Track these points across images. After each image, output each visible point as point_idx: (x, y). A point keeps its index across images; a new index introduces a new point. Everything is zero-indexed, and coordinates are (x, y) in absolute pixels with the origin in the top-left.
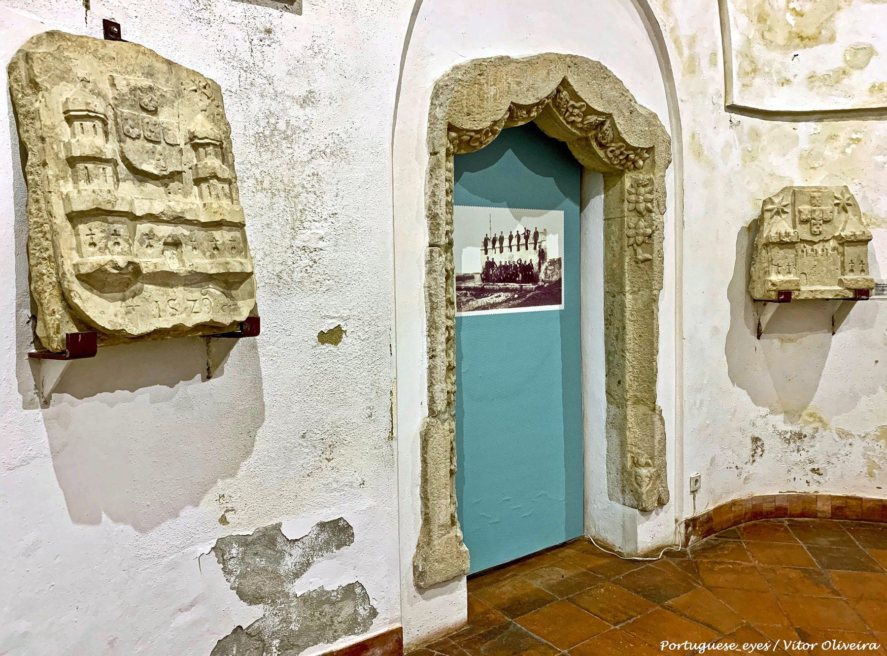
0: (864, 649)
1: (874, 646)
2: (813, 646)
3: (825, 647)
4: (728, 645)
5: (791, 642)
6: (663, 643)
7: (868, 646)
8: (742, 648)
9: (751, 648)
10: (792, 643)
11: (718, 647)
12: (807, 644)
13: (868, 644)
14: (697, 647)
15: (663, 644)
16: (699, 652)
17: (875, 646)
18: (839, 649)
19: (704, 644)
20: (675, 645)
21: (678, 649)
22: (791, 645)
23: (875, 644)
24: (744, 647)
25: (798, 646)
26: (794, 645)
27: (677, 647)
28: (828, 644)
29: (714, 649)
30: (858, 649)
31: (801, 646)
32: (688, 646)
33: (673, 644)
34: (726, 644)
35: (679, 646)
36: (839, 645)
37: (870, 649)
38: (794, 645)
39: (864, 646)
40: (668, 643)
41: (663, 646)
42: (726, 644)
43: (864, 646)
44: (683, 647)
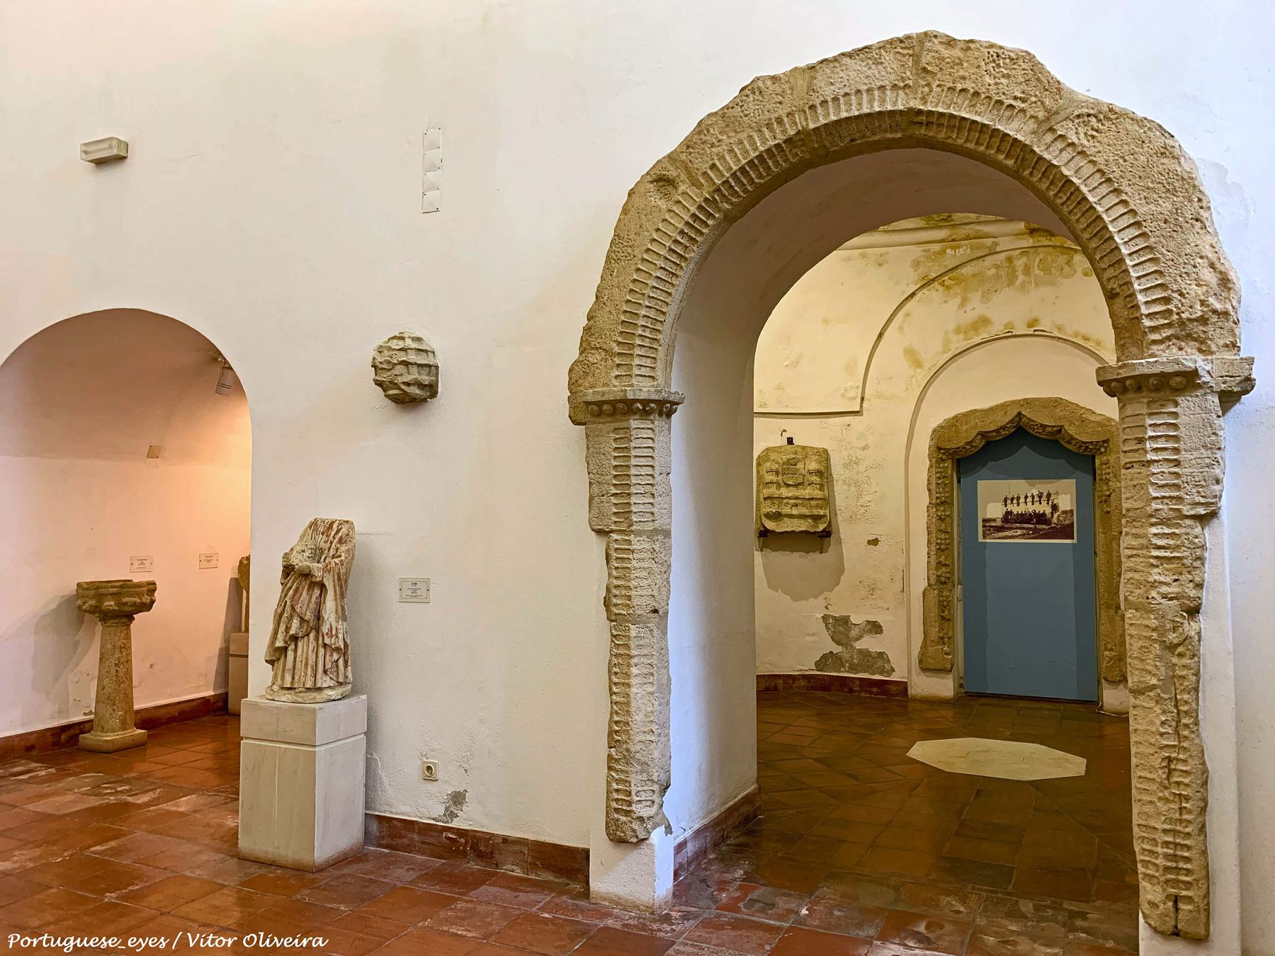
0: (304, 946)
1: (320, 942)
2: (230, 942)
4: (106, 941)
5: (198, 935)
6: (12, 936)
7: (311, 941)
8: (127, 945)
10: (200, 938)
11: (91, 943)
12: (222, 938)
13: (311, 938)
14: (61, 942)
15: (12, 938)
16: (65, 950)
17: (320, 942)
18: (268, 946)
19: (72, 938)
20: (29, 940)
21: (34, 946)
22: (199, 941)
23: (321, 939)
25: (209, 942)
26: (202, 940)
28: (252, 938)
29: (86, 945)
30: (297, 946)
31: (213, 941)
32: (48, 941)
33: (27, 938)
34: (104, 938)
35: (35, 942)
36: (268, 941)
37: (314, 945)
38: (202, 940)
39: (305, 942)
41: (11, 942)
42: (104, 938)
43: (305, 942)
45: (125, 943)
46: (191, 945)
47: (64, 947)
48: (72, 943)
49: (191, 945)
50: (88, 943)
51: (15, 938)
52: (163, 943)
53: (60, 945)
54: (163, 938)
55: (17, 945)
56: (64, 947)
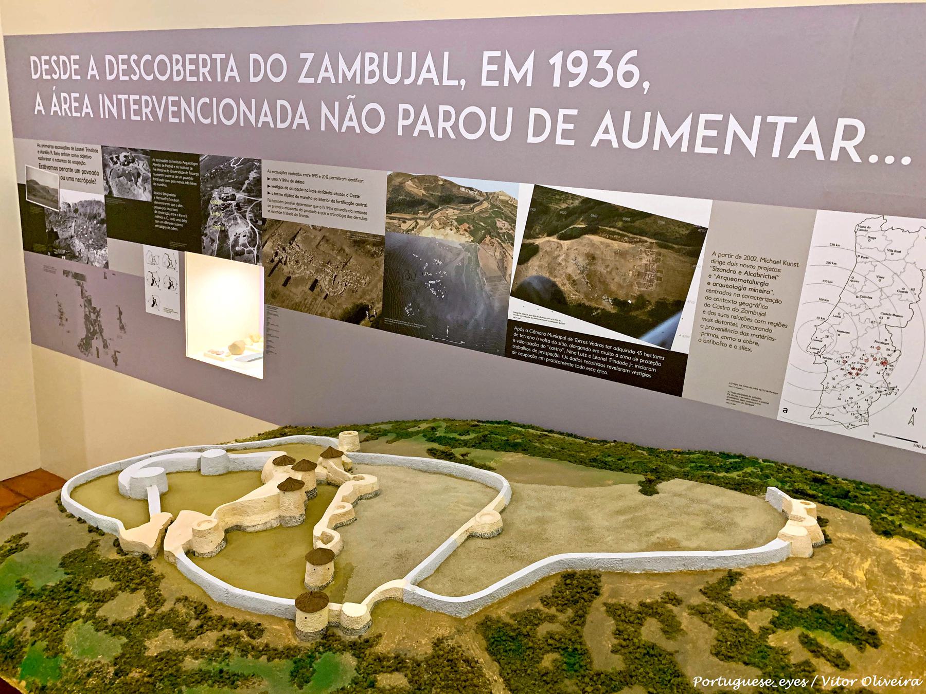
4: (764, 681)
5: (829, 677)
7: (910, 682)
9: (787, 685)
11: (753, 683)
12: (846, 680)
13: (910, 680)
14: (731, 683)
16: (734, 688)
17: (917, 682)
19: (739, 680)
20: (709, 681)
21: (712, 685)
22: (830, 682)
24: (780, 683)
25: (837, 682)
27: (710, 683)
29: (749, 685)
30: (900, 685)
31: (840, 681)
32: (722, 682)
33: (707, 680)
35: (713, 682)
37: (912, 685)
38: (832, 681)
39: (906, 682)
40: (701, 678)
41: (696, 682)
42: (762, 680)
43: (906, 682)
47: (733, 686)
48: (739, 682)
50: (750, 683)
51: (699, 679)
52: (804, 683)
53: (730, 685)
54: (804, 680)
56: (733, 686)
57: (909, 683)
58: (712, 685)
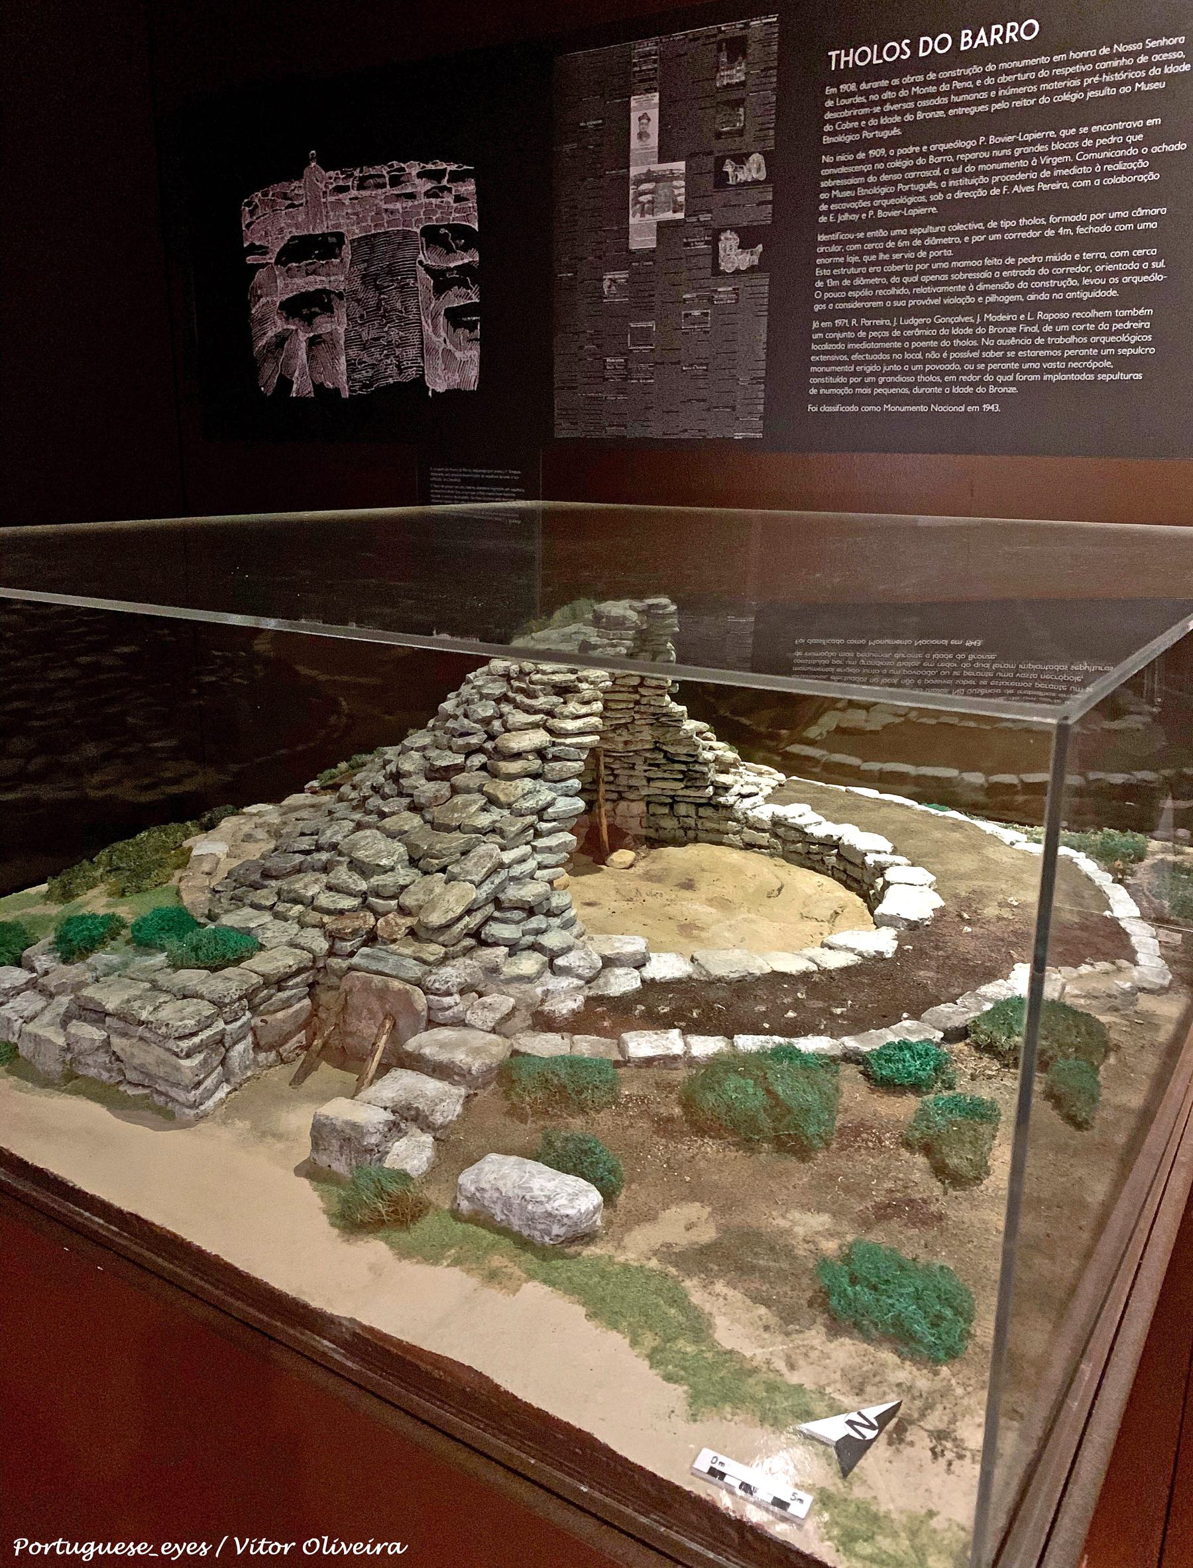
1: (398, 1549)
2: (287, 1548)
3: (308, 1549)
6: (18, 1541)
7: (385, 1549)
8: (160, 1553)
11: (116, 1550)
12: (276, 1543)
14: (79, 1548)
16: (84, 1558)
17: (397, 1549)
19: (92, 1544)
20: (40, 1546)
21: (46, 1552)
22: (249, 1546)
23: (398, 1545)
25: (261, 1548)
28: (314, 1544)
31: (266, 1547)
32: (63, 1547)
33: (37, 1544)
34: (132, 1544)
35: (47, 1548)
36: (333, 1547)
37: (390, 1552)
39: (379, 1548)
40: (27, 1541)
41: (18, 1548)
42: (132, 1544)
43: (379, 1548)
44: (53, 1548)
45: (157, 1549)
46: (239, 1552)
47: (82, 1554)
49: (239, 1552)
50: (112, 1549)
51: (23, 1543)
52: (204, 1550)
54: (204, 1544)
55: (24, 1552)
56: (82, 1554)
57: (385, 1549)
58: (46, 1552)
